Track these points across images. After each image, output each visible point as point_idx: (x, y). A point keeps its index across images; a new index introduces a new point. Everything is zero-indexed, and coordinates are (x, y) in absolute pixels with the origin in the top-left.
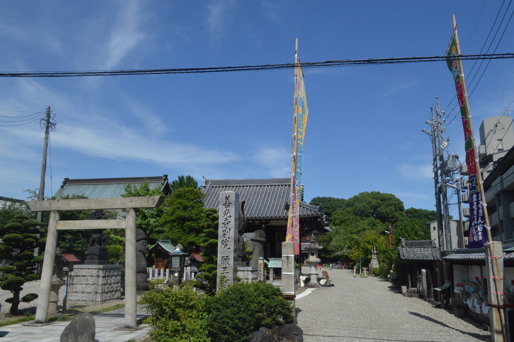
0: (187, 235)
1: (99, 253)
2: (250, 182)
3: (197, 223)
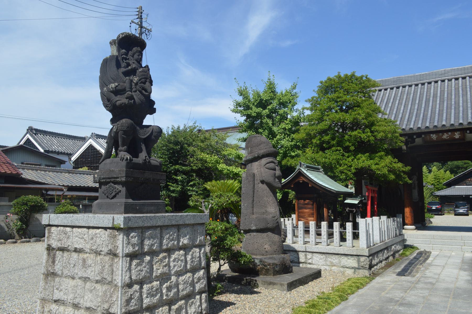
0: (353, 157)
1: (126, 176)
2: (441, 75)
3: (372, 132)
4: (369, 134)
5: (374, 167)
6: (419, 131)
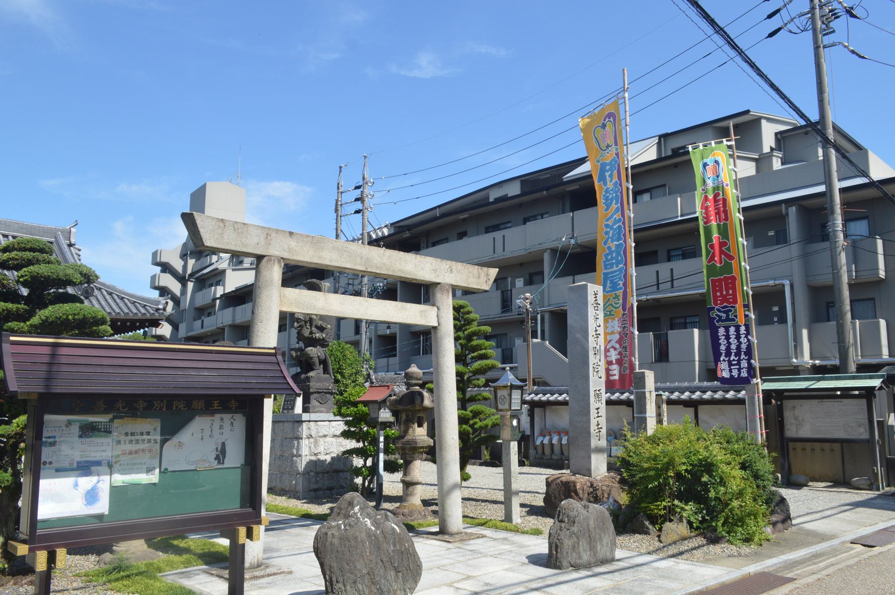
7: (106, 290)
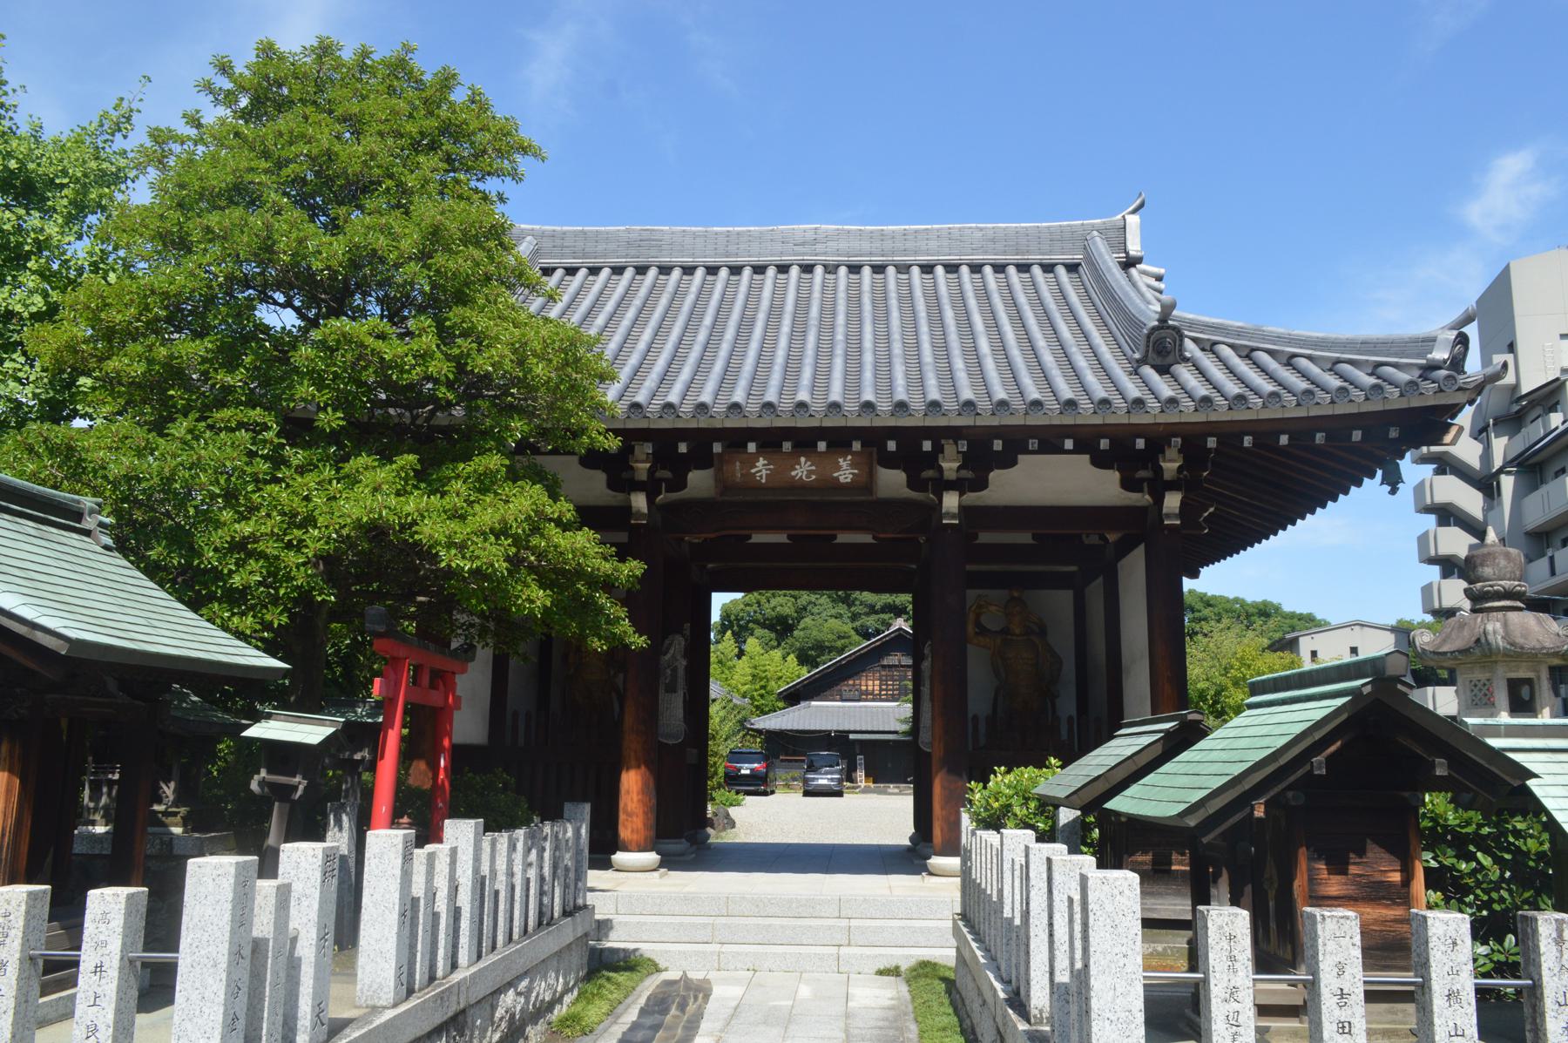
2: (803, 244)
3: (445, 335)
4: (429, 341)
5: (432, 530)
6: (703, 423)
7: (1231, 346)
